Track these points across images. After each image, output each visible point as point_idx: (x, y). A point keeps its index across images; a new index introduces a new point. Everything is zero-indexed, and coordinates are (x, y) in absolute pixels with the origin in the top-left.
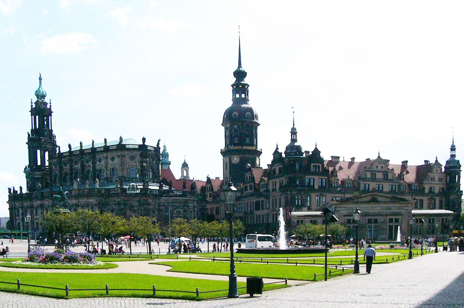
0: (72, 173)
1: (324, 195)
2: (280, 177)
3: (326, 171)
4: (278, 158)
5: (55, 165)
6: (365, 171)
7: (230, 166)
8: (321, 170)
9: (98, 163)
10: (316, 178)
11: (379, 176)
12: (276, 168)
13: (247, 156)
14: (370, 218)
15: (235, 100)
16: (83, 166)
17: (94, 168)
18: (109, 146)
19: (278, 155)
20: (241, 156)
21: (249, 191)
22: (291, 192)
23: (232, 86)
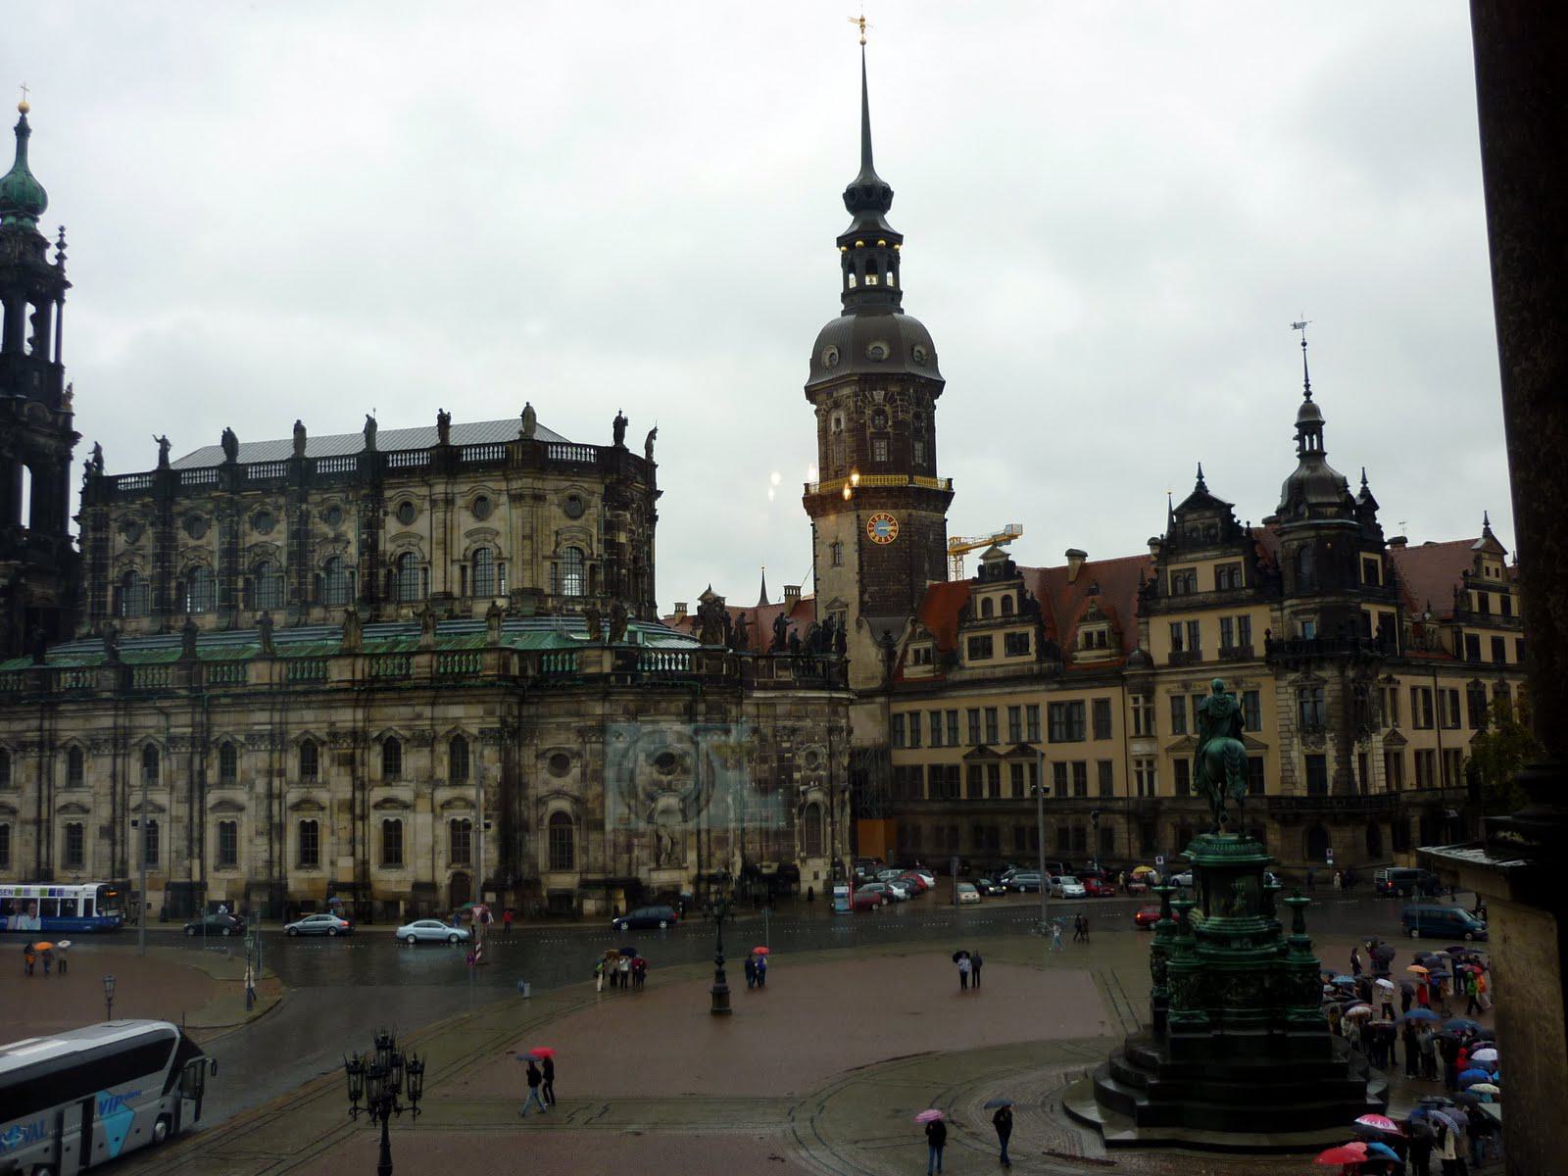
0: (231, 571)
4: (1210, 527)
5: (127, 526)
7: (861, 550)
8: (1381, 583)
9: (392, 526)
10: (1374, 611)
12: (1194, 569)
13: (924, 513)
15: (851, 297)
16: (301, 536)
17: (370, 547)
18: (461, 447)
19: (1208, 514)
22: (1342, 673)
23: (899, 239)
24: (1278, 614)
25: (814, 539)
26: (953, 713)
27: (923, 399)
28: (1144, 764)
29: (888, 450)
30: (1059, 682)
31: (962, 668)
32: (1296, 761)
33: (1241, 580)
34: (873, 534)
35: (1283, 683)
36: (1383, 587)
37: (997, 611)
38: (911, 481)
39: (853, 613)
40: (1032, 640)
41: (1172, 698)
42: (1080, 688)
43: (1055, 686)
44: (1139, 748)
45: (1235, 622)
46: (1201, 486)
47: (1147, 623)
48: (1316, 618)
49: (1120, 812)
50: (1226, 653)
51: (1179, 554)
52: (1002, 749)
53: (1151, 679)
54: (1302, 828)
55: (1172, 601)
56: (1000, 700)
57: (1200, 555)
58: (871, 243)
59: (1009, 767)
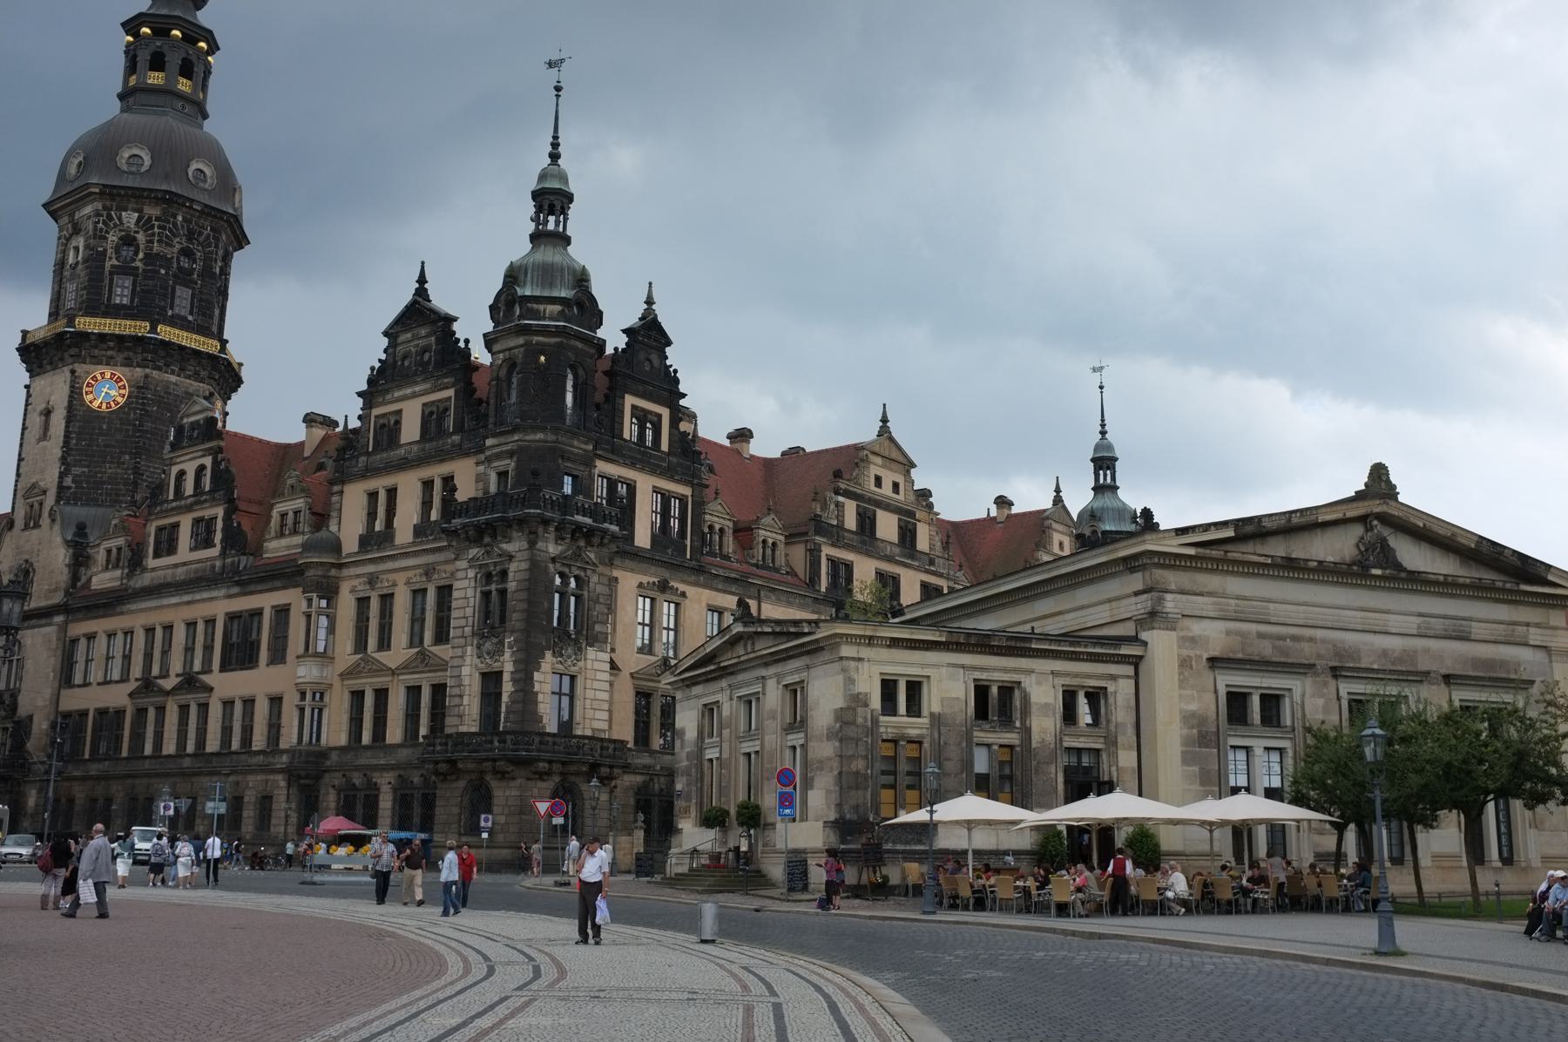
1: (674, 591)
2: (442, 456)
3: (688, 456)
4: (425, 350)
6: (837, 493)
8: (665, 446)
10: (646, 485)
11: (887, 526)
12: (399, 412)
13: (173, 378)
14: (1359, 688)
19: (423, 332)
20: (139, 372)
21: (184, 552)
22: (532, 544)
24: (481, 468)
25: (27, 405)
26: (129, 633)
27: (200, 234)
28: (309, 696)
29: (134, 290)
30: (238, 583)
31: (145, 570)
32: (466, 681)
33: (450, 423)
34: (90, 397)
35: (462, 564)
36: (669, 454)
37: (189, 488)
38: (153, 329)
39: (50, 500)
40: (220, 524)
41: (359, 600)
42: (261, 592)
43: (235, 590)
44: (308, 672)
45: (438, 485)
46: (421, 292)
47: (341, 493)
48: (509, 464)
49: (281, 771)
50: (419, 531)
51: (387, 391)
52: (168, 684)
53: (333, 572)
54: (462, 784)
55: (372, 459)
56: (175, 612)
57: (409, 391)
58: (161, 32)
59: (176, 708)
